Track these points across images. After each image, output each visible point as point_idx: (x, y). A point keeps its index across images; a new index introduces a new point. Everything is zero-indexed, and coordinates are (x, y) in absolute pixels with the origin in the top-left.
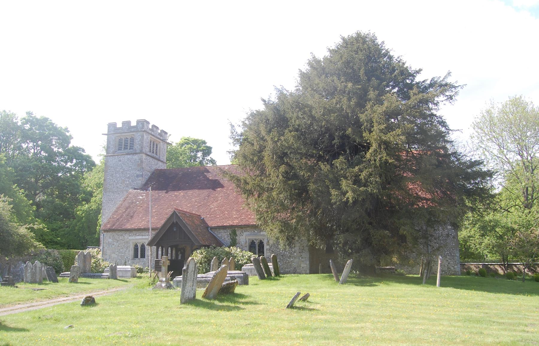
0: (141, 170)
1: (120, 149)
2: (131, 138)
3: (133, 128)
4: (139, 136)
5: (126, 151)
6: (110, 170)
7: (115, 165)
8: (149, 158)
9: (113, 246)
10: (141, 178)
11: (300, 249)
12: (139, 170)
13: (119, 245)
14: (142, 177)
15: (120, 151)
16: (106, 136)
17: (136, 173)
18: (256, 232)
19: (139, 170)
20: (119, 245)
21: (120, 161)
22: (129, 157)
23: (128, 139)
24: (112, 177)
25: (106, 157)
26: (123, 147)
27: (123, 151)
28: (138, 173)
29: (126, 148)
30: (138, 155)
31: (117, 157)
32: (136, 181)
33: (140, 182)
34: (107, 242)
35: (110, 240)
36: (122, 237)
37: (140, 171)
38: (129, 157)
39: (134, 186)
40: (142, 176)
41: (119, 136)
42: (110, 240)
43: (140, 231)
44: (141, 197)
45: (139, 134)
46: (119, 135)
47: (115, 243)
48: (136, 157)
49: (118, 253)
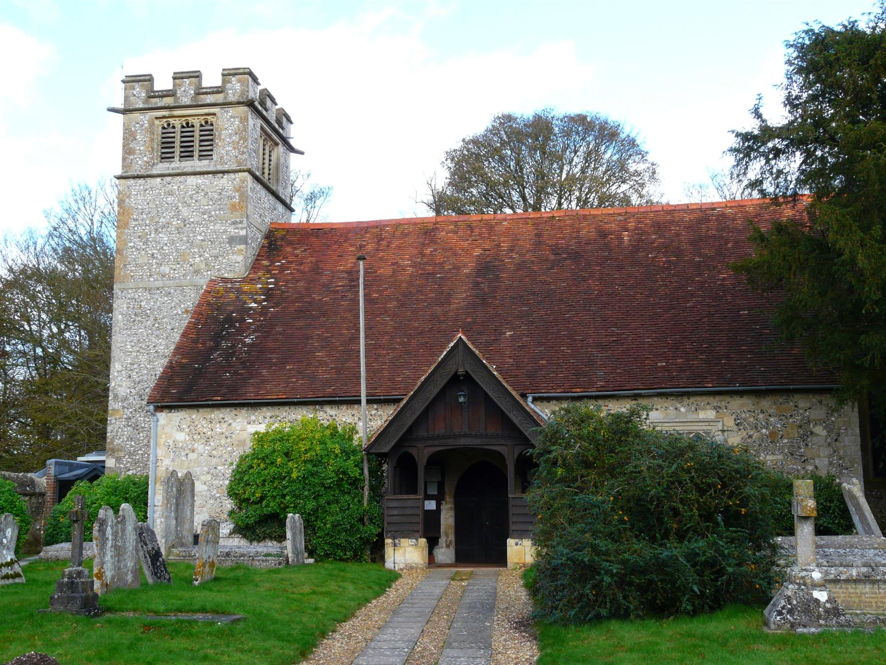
0: (241, 222)
1: (166, 157)
2: (202, 125)
3: (213, 93)
4: (231, 117)
5: (188, 165)
6: (137, 220)
7: (152, 205)
8: (259, 187)
9: (192, 456)
10: (242, 247)
11: (831, 463)
12: (234, 223)
13: (214, 452)
14: (246, 243)
15: (166, 165)
16: (120, 117)
17: (225, 231)
18: (683, 410)
19: (234, 223)
20: (214, 452)
21: (170, 193)
22: (200, 181)
23: (193, 126)
24: (145, 243)
25: (122, 181)
26: (177, 150)
27: (177, 165)
28: (232, 230)
29: (187, 154)
30: (232, 176)
31: (159, 180)
32: (228, 254)
33: (240, 258)
34: (171, 442)
35: (181, 437)
36: (225, 426)
37: (240, 226)
38: (200, 181)
39: (219, 270)
40: (244, 240)
41: (164, 117)
42: (181, 437)
43: (287, 408)
44: (253, 305)
45: (231, 111)
46: (165, 113)
47: (199, 447)
48: (224, 181)
49: (209, 477)
